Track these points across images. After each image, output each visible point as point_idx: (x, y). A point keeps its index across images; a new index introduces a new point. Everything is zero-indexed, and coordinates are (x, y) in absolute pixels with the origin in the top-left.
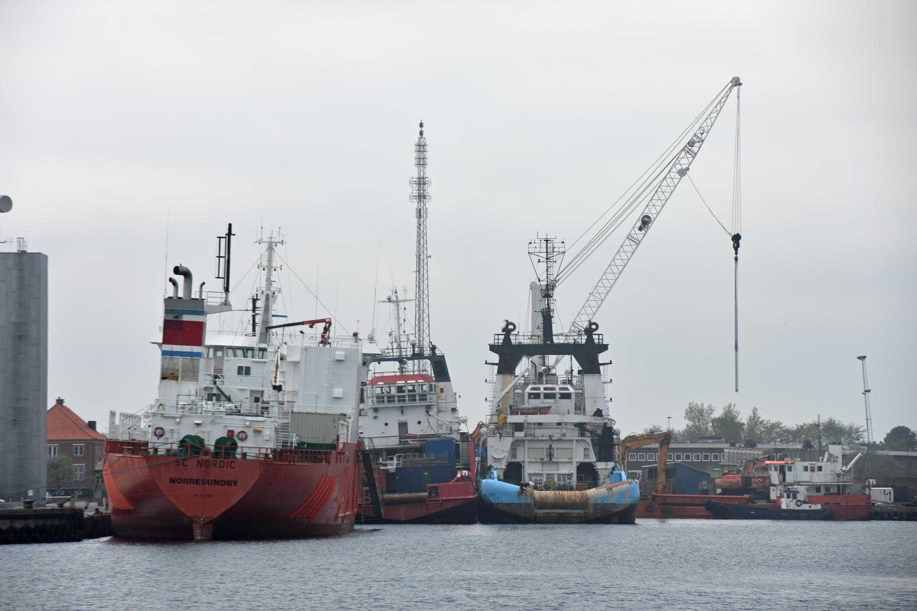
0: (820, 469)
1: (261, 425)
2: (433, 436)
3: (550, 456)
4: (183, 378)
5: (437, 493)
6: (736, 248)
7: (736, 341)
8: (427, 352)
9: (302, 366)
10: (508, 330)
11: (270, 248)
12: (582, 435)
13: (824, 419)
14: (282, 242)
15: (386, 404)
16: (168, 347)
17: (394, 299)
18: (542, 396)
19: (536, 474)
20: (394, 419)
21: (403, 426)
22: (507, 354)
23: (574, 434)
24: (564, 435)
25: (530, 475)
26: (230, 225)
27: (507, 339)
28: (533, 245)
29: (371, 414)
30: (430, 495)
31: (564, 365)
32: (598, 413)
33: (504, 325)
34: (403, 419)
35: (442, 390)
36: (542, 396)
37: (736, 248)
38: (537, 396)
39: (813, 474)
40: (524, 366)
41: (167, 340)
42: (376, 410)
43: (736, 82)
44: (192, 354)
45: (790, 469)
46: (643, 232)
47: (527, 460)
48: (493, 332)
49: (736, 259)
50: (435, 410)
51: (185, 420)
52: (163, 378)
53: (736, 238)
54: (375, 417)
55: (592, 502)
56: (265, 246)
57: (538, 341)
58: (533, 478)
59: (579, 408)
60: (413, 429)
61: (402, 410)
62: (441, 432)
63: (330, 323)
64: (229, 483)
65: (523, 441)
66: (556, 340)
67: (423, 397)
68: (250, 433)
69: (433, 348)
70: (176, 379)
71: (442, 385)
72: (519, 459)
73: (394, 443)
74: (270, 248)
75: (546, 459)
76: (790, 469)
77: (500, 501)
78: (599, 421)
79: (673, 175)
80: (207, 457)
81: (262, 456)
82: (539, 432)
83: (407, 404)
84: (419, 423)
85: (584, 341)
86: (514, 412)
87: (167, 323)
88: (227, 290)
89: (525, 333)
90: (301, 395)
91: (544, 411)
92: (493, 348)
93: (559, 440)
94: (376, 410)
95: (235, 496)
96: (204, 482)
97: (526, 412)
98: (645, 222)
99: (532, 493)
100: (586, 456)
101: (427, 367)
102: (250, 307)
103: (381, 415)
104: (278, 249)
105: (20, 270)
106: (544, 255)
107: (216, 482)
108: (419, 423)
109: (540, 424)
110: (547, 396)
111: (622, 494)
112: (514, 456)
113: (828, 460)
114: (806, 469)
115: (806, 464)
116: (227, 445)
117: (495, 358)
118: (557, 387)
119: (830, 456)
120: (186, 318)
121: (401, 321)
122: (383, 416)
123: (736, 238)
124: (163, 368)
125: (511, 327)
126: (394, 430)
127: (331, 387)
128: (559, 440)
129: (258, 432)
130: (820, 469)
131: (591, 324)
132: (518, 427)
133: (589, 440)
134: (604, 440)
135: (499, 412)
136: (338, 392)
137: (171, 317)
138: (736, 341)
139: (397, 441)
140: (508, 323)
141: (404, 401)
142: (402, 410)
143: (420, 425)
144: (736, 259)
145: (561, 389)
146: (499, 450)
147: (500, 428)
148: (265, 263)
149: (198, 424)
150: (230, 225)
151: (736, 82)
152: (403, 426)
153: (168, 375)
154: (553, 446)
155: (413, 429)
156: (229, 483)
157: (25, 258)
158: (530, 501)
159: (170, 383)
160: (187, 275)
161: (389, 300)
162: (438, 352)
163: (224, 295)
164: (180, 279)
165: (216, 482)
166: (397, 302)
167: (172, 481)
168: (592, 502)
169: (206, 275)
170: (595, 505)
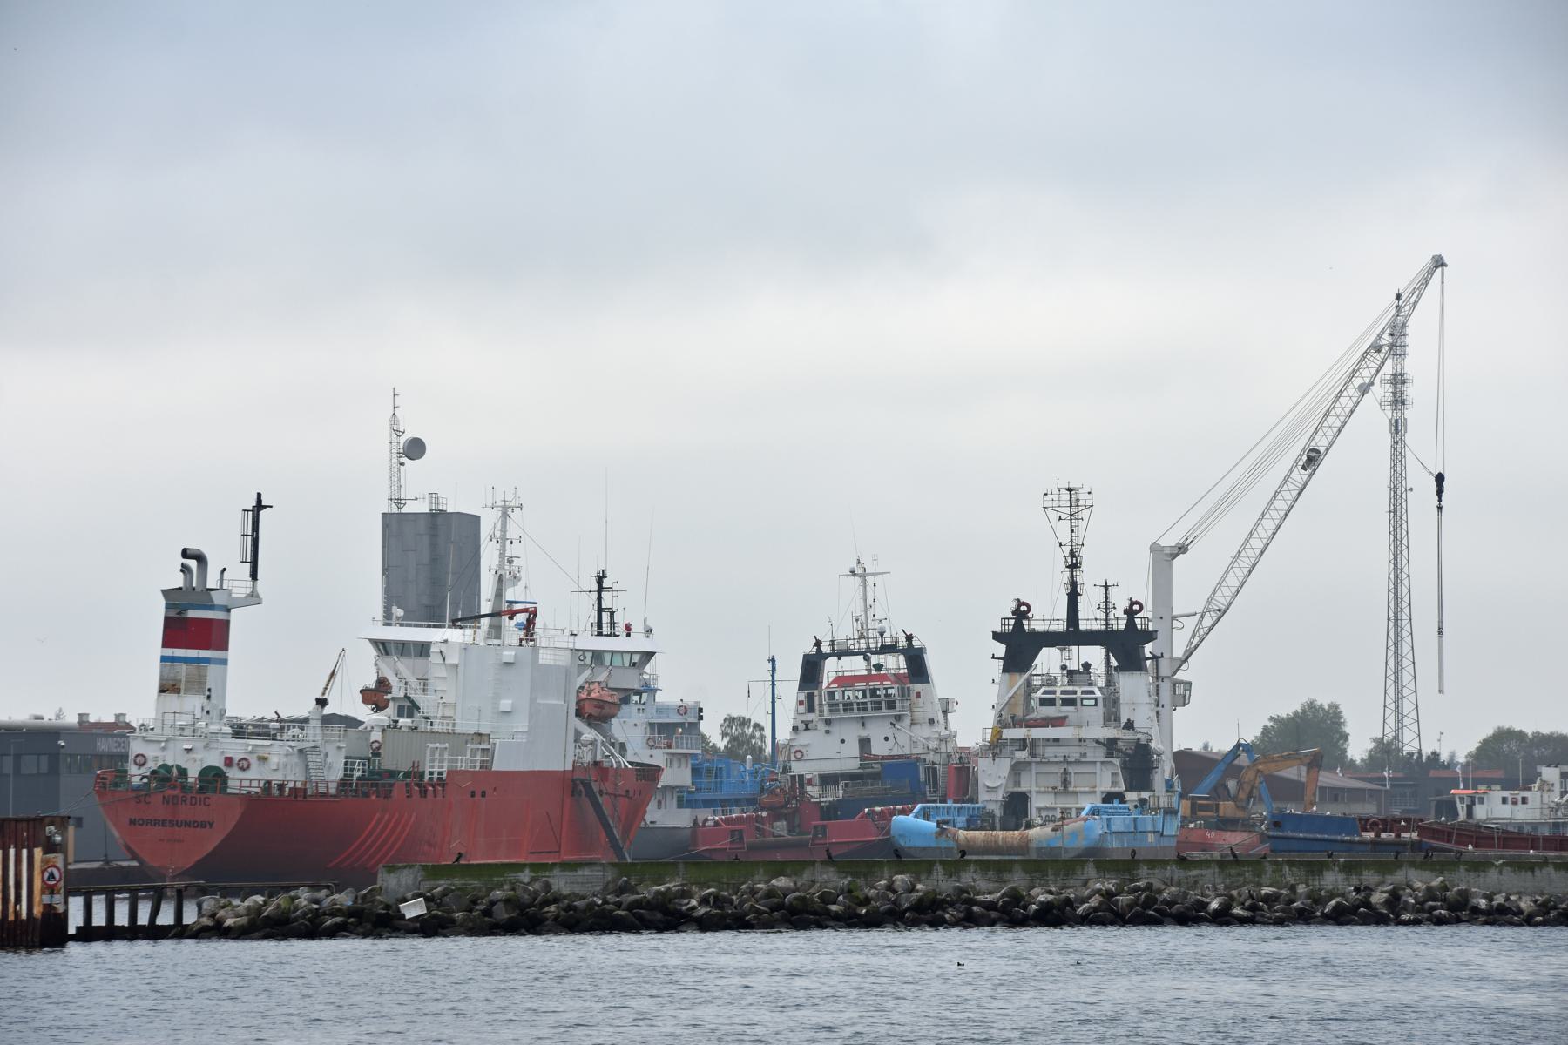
0: (1524, 800)
1: (267, 750)
2: (900, 756)
3: (1066, 783)
4: (186, 691)
5: (824, 834)
6: (1440, 492)
7: (1441, 622)
8: (902, 643)
9: (461, 669)
10: (1021, 613)
11: (505, 515)
12: (1110, 755)
13: (1517, 728)
14: (521, 507)
15: (842, 715)
16: (169, 652)
17: (859, 571)
18: (1059, 702)
19: (1046, 809)
20: (852, 733)
21: (865, 743)
22: (1019, 644)
23: (1099, 754)
24: (1084, 755)
25: (1039, 809)
26: (259, 495)
27: (1018, 625)
28: (1049, 497)
29: (822, 727)
30: (815, 836)
31: (1095, 655)
32: (1130, 725)
33: (1014, 605)
34: (864, 734)
35: (918, 695)
36: (1059, 702)
37: (1440, 492)
38: (1051, 702)
39: (1516, 808)
40: (1048, 660)
41: (166, 643)
42: (828, 722)
43: (1439, 263)
44: (198, 660)
45: (1482, 801)
46: (1309, 471)
47: (1034, 789)
48: (999, 615)
49: (1440, 508)
50: (907, 721)
51: (171, 745)
52: (162, 691)
53: (1440, 479)
54: (827, 732)
55: (1034, 845)
56: (498, 513)
57: (1061, 627)
58: (1044, 814)
59: (1111, 717)
60: (879, 748)
61: (863, 722)
62: (915, 751)
63: (535, 614)
64: (203, 825)
65: (1030, 763)
66: (1082, 627)
67: (891, 705)
68: (253, 760)
69: (909, 638)
70: (178, 691)
71: (917, 687)
72: (1023, 788)
73: (852, 766)
74: (505, 515)
75: (1060, 788)
76: (1482, 801)
77: (911, 844)
78: (1129, 735)
79: (1351, 391)
80: (176, 792)
81: (786, 780)
82: (1051, 752)
83: (870, 713)
84: (886, 739)
85: (1122, 627)
86: (1016, 723)
87: (168, 621)
88: (254, 575)
89: (1049, 614)
90: (459, 707)
91: (1059, 722)
92: (997, 636)
93: (1078, 762)
94: (828, 722)
95: (212, 840)
96: (173, 824)
97: (1031, 725)
98: (1312, 459)
99: (955, 835)
100: (1114, 784)
101: (895, 663)
102: (595, 587)
103: (834, 728)
104: (515, 515)
105: (434, 536)
106: (1067, 510)
107: (187, 824)
108: (886, 739)
109: (1056, 740)
110: (1066, 702)
111: (1074, 834)
112: (1018, 784)
113: (1541, 788)
114: (1504, 800)
115: (1506, 794)
116: (213, 778)
117: (1000, 649)
118: (1058, 690)
119: (1544, 782)
120: (192, 614)
121: (870, 601)
122: (839, 731)
123: (1440, 479)
124: (162, 679)
125: (1136, 607)
126: (853, 749)
127: (497, 697)
128: (1078, 762)
129: (263, 759)
130: (1524, 800)
131: (1132, 603)
132: (1022, 744)
133: (1117, 762)
134: (1137, 763)
135: (1002, 724)
136: (506, 704)
137: (173, 614)
138: (1441, 622)
139: (857, 763)
140: (1021, 603)
141: (865, 709)
142: (863, 722)
143: (887, 741)
144: (1440, 508)
145: (1063, 692)
146: (993, 779)
147: (996, 746)
148: (498, 534)
149: (188, 750)
150: (259, 495)
151: (1439, 263)
152: (865, 743)
153: (168, 687)
154: (1070, 770)
155: (879, 748)
156: (203, 825)
157: (440, 520)
158: (952, 844)
159: (169, 697)
160: (201, 558)
161: (853, 573)
162: (916, 643)
163: (250, 584)
164: (193, 564)
165: (187, 824)
166: (864, 576)
167: (132, 822)
168: (1034, 845)
169: (225, 559)
170: (1039, 850)
